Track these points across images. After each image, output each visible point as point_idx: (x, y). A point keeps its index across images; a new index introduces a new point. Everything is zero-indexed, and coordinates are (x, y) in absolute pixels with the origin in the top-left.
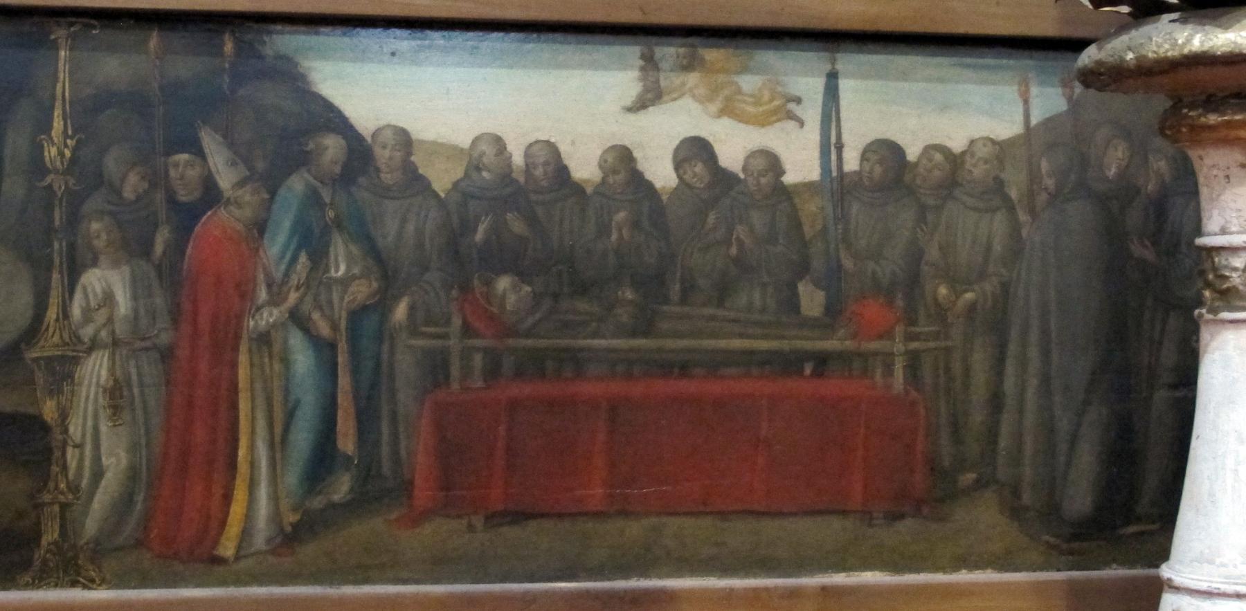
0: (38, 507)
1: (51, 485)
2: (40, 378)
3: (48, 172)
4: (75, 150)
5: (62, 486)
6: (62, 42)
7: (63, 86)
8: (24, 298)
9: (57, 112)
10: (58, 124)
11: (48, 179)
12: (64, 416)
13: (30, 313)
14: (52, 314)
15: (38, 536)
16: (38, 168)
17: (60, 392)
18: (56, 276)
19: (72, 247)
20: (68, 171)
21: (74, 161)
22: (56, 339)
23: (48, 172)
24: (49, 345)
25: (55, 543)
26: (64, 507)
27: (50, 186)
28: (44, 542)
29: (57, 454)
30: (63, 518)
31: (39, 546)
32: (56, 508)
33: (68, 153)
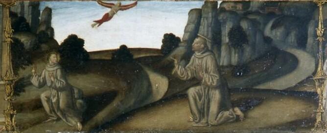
0: (315, 113)
1: (319, 108)
2: (317, 84)
3: (318, 36)
4: (324, 31)
5: (322, 108)
6: (320, 7)
7: (321, 17)
8: (314, 65)
9: (320, 23)
10: (320, 26)
11: (318, 38)
12: (322, 92)
13: (314, 69)
14: (319, 69)
15: (315, 120)
16: (316, 36)
17: (321, 87)
18: (320, 60)
19: (324, 53)
20: (322, 36)
21: (324, 33)
22: (320, 75)
23: (318, 36)
24: (319, 76)
25: (320, 122)
26: (322, 113)
27: (318, 40)
28: (317, 121)
29: (320, 101)
30: (322, 116)
31: (316, 122)
32: (320, 113)
33: (322, 32)
